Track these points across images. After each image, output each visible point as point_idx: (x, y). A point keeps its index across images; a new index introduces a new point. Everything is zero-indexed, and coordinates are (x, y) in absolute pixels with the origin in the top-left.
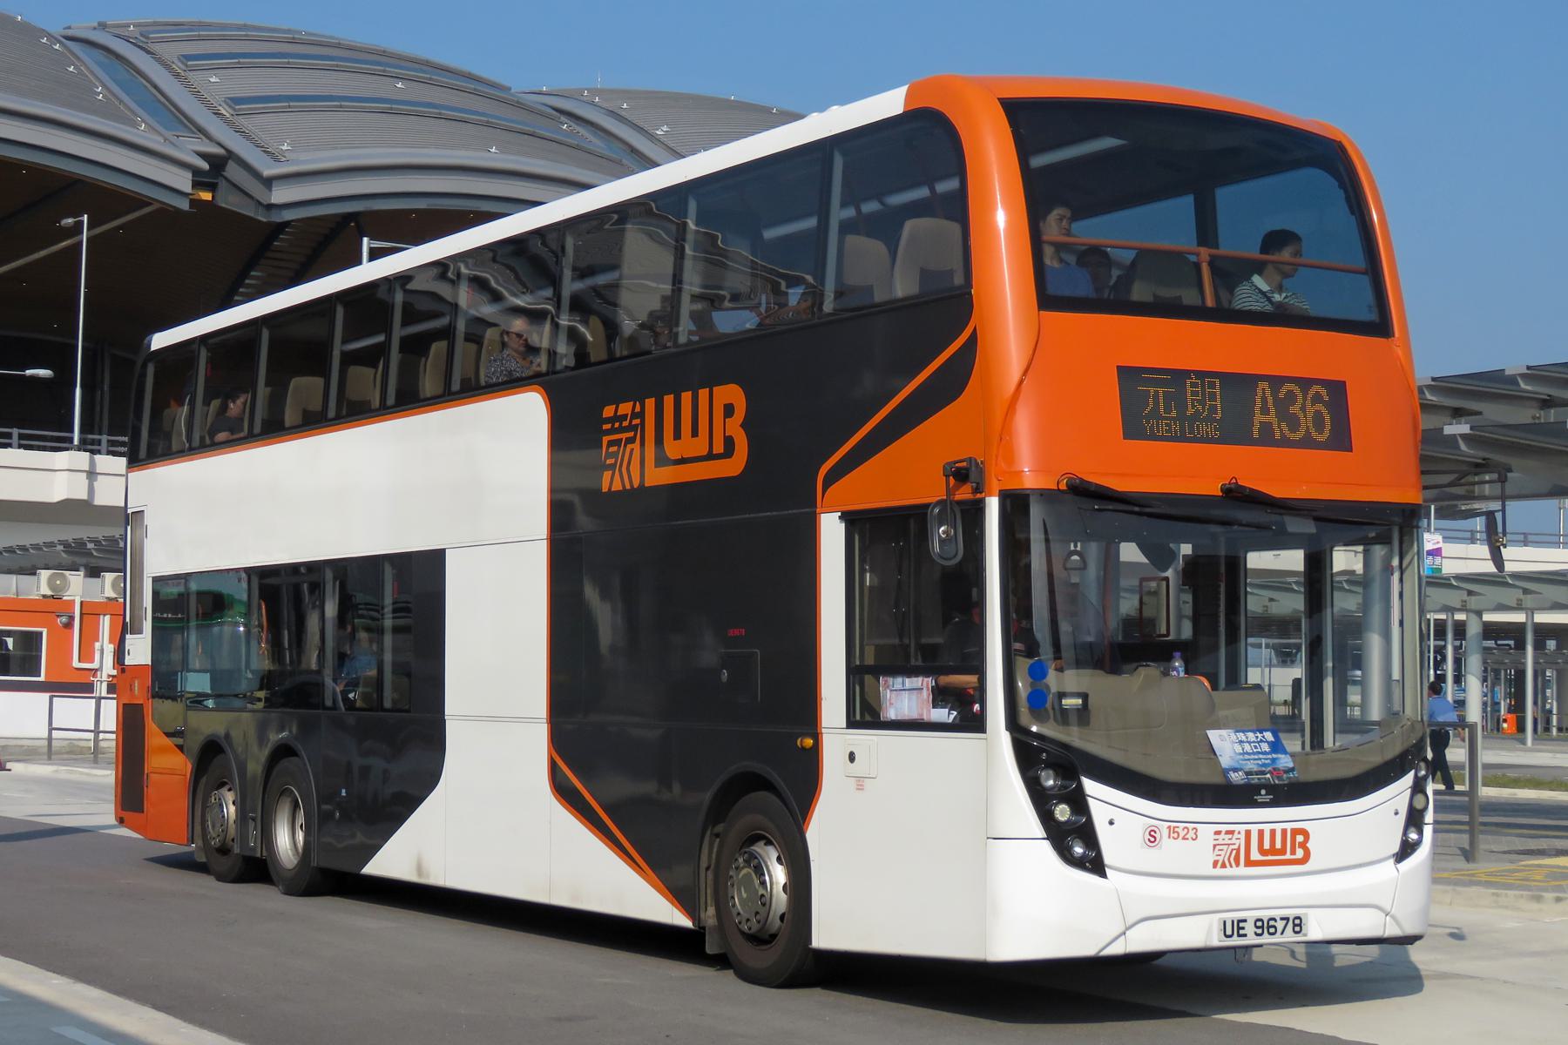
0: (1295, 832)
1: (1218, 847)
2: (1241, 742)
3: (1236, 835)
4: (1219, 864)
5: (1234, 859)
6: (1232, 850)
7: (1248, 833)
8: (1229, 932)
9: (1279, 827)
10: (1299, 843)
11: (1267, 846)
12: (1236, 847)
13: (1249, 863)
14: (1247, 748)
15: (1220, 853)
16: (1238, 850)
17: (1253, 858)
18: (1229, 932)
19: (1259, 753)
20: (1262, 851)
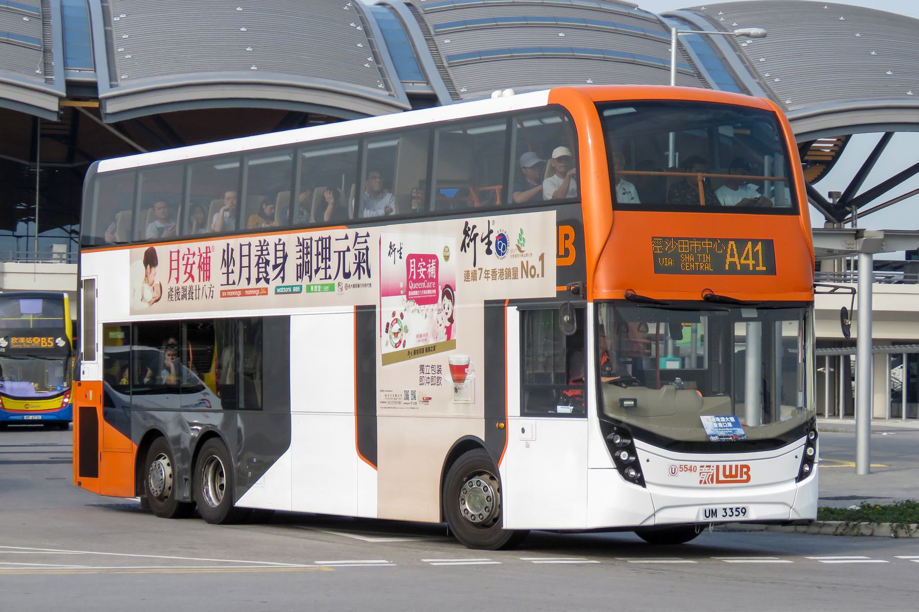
0: (743, 467)
1: (702, 474)
2: (717, 422)
3: (711, 468)
4: (703, 482)
5: (711, 479)
6: (710, 475)
7: (718, 467)
8: (708, 515)
9: (734, 464)
10: (745, 472)
11: (727, 473)
12: (711, 474)
13: (718, 482)
14: (720, 425)
15: (703, 476)
16: (713, 475)
17: (720, 479)
18: (708, 515)
19: (726, 427)
20: (725, 476)
